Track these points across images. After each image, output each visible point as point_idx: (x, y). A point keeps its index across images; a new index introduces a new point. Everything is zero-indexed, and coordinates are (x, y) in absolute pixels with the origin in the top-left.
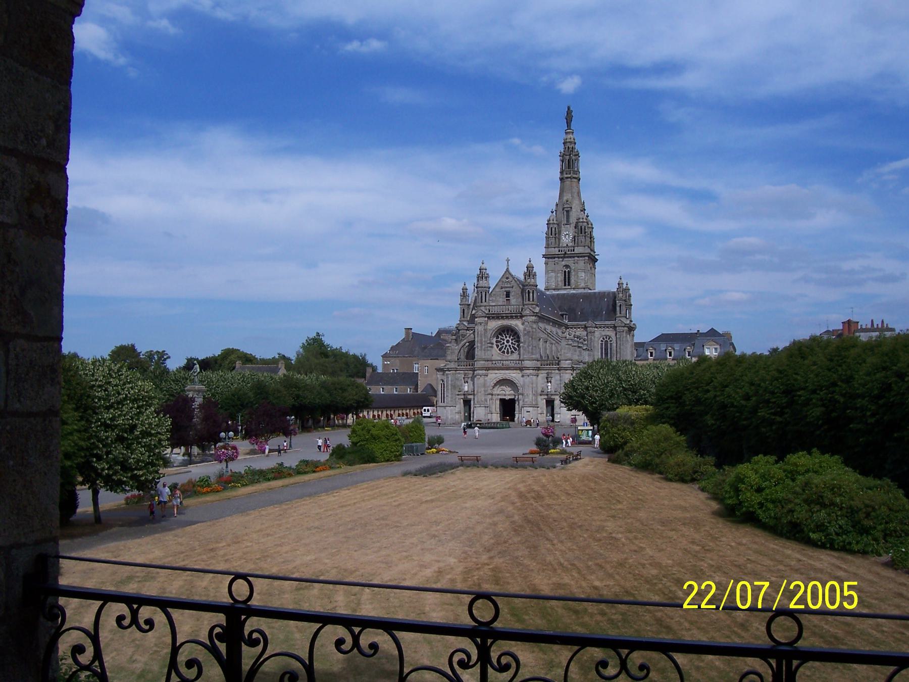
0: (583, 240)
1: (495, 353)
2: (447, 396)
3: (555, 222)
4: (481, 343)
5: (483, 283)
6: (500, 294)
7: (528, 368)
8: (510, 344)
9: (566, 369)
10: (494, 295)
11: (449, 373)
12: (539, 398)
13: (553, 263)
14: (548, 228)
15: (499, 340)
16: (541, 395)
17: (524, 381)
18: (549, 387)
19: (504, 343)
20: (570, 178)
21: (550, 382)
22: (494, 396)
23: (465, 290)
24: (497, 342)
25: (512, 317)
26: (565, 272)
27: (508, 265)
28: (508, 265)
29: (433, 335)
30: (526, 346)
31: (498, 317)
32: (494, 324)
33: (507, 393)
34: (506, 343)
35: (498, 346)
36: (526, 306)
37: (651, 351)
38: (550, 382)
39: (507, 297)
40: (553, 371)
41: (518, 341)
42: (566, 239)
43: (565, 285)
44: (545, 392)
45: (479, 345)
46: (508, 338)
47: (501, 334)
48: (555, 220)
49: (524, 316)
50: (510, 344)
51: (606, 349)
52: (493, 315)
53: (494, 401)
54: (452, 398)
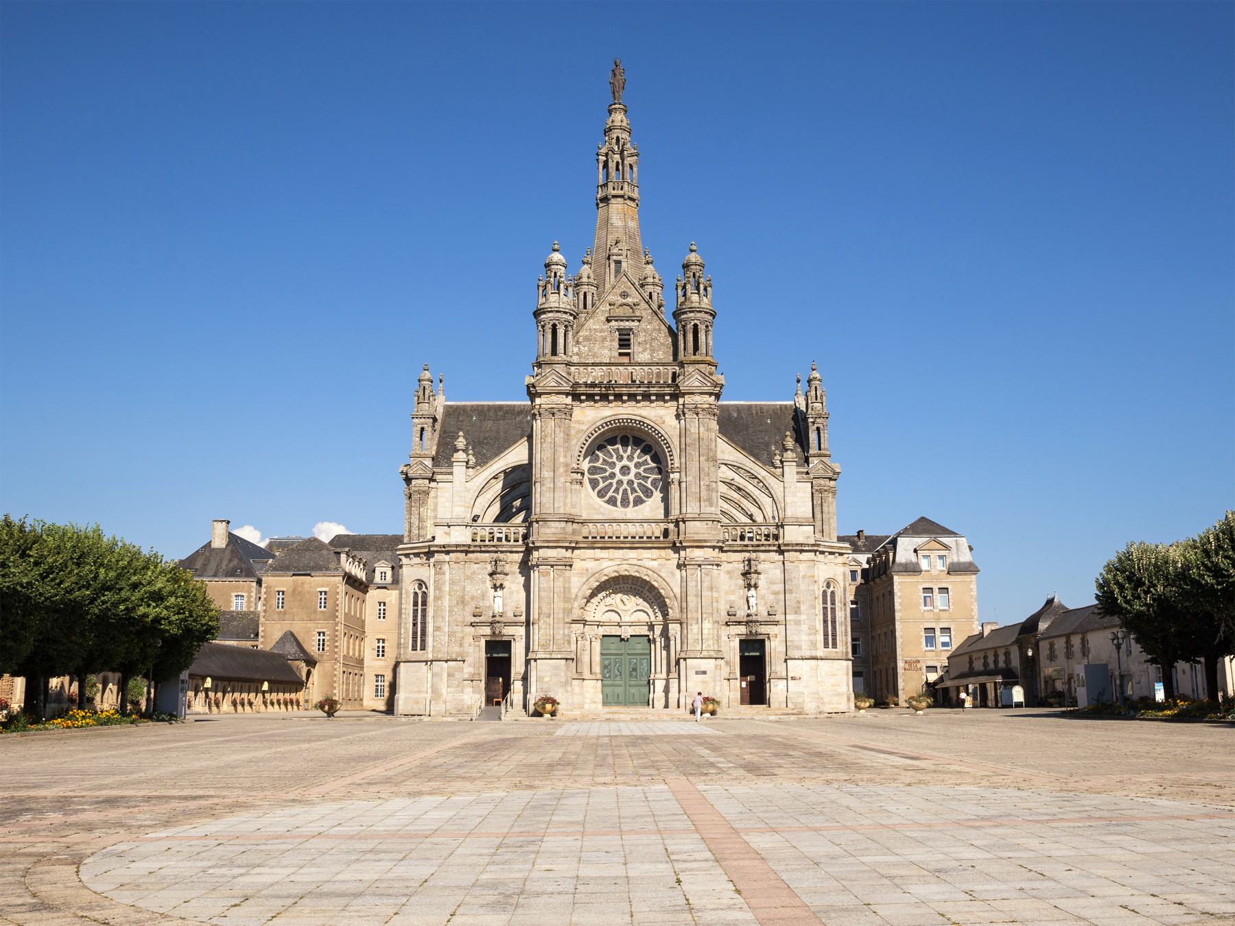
1: (588, 503)
2: (437, 629)
3: (591, 280)
6: (604, 339)
8: (631, 476)
9: (800, 548)
10: (587, 339)
11: (447, 558)
12: (725, 631)
16: (727, 624)
17: (684, 582)
18: (752, 601)
19: (613, 476)
20: (622, 197)
21: (756, 586)
24: (593, 470)
25: (646, 397)
31: (604, 393)
32: (591, 417)
33: (626, 618)
34: (619, 476)
35: (594, 484)
36: (690, 369)
39: (621, 346)
40: (762, 556)
44: (741, 614)
48: (592, 276)
49: (683, 395)
50: (631, 476)
52: (590, 391)
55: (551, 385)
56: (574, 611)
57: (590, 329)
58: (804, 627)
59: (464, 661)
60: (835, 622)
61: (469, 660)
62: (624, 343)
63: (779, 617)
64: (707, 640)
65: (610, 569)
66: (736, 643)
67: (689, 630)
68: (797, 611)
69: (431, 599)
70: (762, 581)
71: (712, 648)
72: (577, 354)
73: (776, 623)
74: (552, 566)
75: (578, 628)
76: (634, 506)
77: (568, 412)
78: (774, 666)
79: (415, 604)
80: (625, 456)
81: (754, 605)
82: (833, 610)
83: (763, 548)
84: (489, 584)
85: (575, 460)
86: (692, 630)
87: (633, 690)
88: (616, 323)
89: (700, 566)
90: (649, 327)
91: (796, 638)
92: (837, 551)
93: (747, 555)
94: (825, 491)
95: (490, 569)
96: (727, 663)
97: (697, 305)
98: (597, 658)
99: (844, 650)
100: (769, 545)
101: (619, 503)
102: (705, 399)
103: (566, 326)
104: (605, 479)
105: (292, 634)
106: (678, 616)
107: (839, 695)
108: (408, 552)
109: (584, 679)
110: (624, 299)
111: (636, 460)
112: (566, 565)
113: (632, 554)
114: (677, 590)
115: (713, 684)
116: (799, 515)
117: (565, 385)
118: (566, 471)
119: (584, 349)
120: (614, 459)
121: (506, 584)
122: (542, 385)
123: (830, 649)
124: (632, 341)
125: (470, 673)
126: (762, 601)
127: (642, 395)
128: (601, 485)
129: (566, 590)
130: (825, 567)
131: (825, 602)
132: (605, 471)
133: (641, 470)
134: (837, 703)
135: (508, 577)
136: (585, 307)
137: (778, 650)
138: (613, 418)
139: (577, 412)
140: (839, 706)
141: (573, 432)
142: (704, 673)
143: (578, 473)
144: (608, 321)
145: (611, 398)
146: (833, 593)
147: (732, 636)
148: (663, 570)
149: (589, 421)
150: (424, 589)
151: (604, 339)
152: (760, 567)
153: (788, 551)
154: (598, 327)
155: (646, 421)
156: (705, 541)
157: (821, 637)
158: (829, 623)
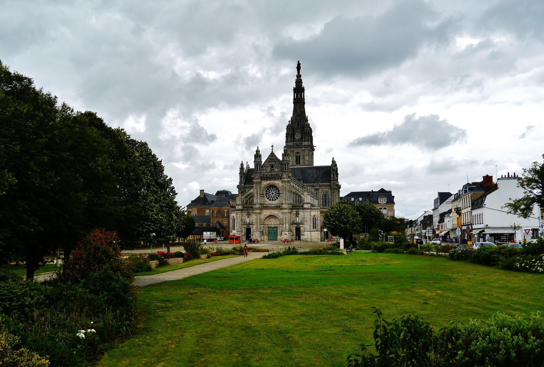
2: (237, 226)
4: (257, 194)
5: (258, 160)
6: (268, 166)
7: (285, 209)
8: (274, 195)
9: (307, 209)
10: (265, 166)
14: (287, 131)
18: (298, 220)
19: (270, 195)
20: (300, 102)
21: (298, 217)
23: (242, 165)
24: (266, 194)
25: (275, 179)
27: (272, 149)
28: (272, 149)
29: (214, 194)
32: (265, 183)
34: (271, 195)
35: (267, 196)
40: (300, 211)
41: (279, 193)
42: (298, 136)
43: (297, 164)
44: (295, 222)
45: (256, 195)
46: (273, 192)
47: (268, 189)
50: (274, 195)
51: (326, 199)
54: (239, 227)
58: (308, 225)
61: (243, 232)
62: (272, 166)
63: (303, 223)
66: (295, 228)
68: (307, 222)
69: (235, 220)
70: (300, 216)
73: (303, 224)
75: (263, 226)
77: (260, 183)
78: (302, 233)
82: (315, 221)
84: (246, 217)
87: (274, 237)
96: (293, 232)
98: (267, 231)
104: (269, 195)
105: (218, 222)
113: (273, 211)
114: (282, 218)
128: (268, 197)
129: (260, 218)
131: (313, 219)
139: (262, 182)
144: (269, 162)
146: (315, 218)
151: (268, 166)
152: (300, 213)
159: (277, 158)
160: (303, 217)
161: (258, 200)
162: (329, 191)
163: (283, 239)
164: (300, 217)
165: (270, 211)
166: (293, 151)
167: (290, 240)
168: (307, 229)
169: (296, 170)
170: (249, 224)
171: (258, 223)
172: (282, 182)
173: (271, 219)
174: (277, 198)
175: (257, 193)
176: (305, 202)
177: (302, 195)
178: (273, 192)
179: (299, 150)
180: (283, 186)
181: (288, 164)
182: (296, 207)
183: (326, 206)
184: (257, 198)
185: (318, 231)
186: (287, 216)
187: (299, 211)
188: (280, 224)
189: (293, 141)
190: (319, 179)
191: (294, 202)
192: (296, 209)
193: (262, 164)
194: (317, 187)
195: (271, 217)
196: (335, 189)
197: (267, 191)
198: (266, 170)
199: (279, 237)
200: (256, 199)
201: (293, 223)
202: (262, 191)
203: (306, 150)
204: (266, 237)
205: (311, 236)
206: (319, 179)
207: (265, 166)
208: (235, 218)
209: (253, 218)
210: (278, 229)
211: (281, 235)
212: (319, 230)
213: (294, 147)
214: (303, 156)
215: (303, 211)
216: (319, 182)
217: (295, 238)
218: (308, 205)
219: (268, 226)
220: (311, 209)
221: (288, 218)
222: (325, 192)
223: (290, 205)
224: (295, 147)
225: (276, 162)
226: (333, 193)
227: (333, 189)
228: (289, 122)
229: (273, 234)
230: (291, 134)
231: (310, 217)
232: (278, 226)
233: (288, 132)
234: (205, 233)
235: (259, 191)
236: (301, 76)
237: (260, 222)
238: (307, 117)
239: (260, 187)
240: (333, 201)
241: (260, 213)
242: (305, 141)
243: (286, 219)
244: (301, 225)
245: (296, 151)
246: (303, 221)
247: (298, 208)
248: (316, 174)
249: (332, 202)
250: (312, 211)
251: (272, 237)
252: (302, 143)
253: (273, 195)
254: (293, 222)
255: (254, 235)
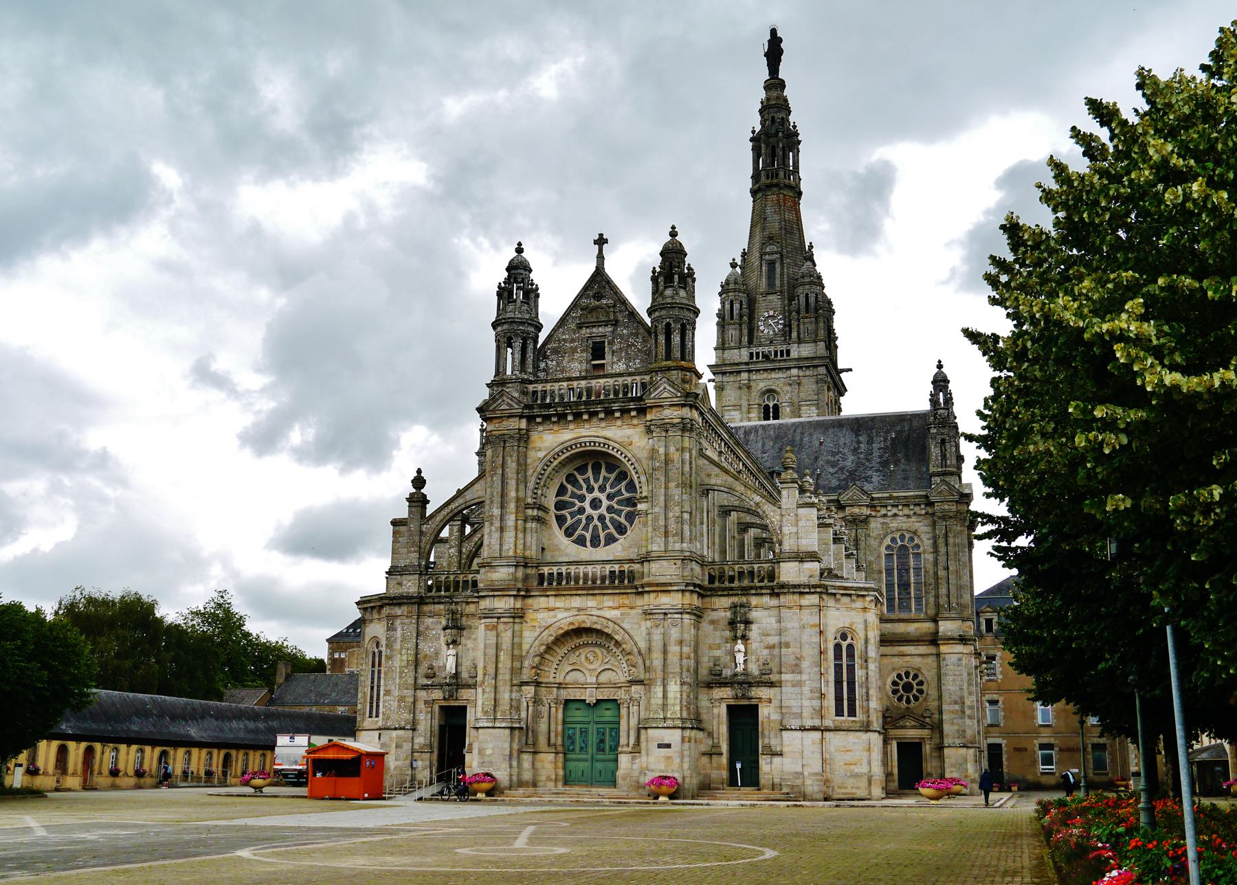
0: (811, 327)
4: (502, 507)
7: (663, 588)
8: (603, 510)
9: (798, 589)
13: (737, 385)
14: (723, 303)
15: (566, 498)
18: (740, 658)
19: (582, 510)
20: (777, 185)
21: (744, 638)
22: (543, 691)
24: (560, 506)
25: (609, 413)
26: (767, 407)
27: (600, 257)
28: (600, 257)
30: (656, 509)
34: (589, 511)
35: (561, 520)
37: (988, 616)
38: (744, 638)
40: (754, 601)
42: (769, 326)
44: (727, 673)
45: (496, 511)
46: (596, 494)
47: (571, 479)
50: (603, 510)
53: (544, 710)
54: (402, 699)
55: (502, 408)
56: (525, 671)
57: (559, 340)
58: (806, 690)
59: (414, 730)
60: (854, 683)
62: (598, 351)
63: (774, 677)
64: (674, 705)
65: (564, 621)
66: (723, 710)
67: (652, 694)
68: (796, 668)
70: (754, 632)
71: (679, 716)
72: (544, 370)
73: (771, 684)
74: (499, 618)
75: (529, 691)
76: (605, 546)
77: (523, 438)
78: (768, 738)
79: (373, 666)
80: (596, 486)
81: (742, 662)
82: (851, 669)
83: (753, 592)
84: (443, 640)
85: (530, 493)
86: (655, 693)
87: (599, 766)
88: (588, 331)
89: (665, 614)
90: (625, 332)
91: (793, 703)
92: (853, 592)
93: (735, 599)
94: (950, 518)
95: (444, 623)
97: (669, 300)
99: (865, 719)
100: (761, 588)
101: (588, 543)
102: (675, 413)
103: (525, 340)
104: (572, 515)
106: (642, 677)
107: (856, 776)
108: (365, 606)
109: (535, 753)
110: (598, 301)
111: (608, 490)
112: (514, 617)
113: (591, 602)
114: (642, 645)
115: (678, 760)
116: (803, 549)
117: (516, 406)
118: (517, 507)
119: (551, 364)
120: (584, 491)
121: (463, 640)
122: (491, 408)
123: (845, 718)
124: (606, 349)
125: (420, 744)
126: (753, 657)
127: (557, 415)
128: (569, 521)
129: (516, 645)
130: (837, 613)
131: (838, 656)
132: (573, 505)
133: (613, 503)
134: (852, 788)
135: (465, 633)
136: (732, 318)
137: (772, 718)
138: (573, 442)
139: (534, 436)
140: (854, 791)
141: (529, 461)
142: (668, 746)
143: (533, 508)
145: (570, 418)
146: (850, 647)
147: (716, 700)
148: (626, 620)
149: (546, 448)
150: (380, 648)
151: (574, 350)
152: (754, 615)
153: (785, 593)
154: (567, 336)
155: (611, 443)
156: (670, 584)
157: (830, 701)
158: (845, 684)
159: (623, 302)
160: (773, 640)
161: (510, 536)
162: (922, 527)
163: (647, 780)
164: (754, 645)
165: (577, 602)
166: (749, 387)
167: (691, 782)
168: (800, 716)
169: (752, 436)
170: (456, 683)
171: (505, 675)
172: (649, 431)
173: (584, 652)
174: (621, 530)
175: (503, 495)
176: (787, 547)
177: (768, 508)
178: (596, 494)
179: (776, 380)
180: (653, 451)
181: (683, 326)
182: (732, 579)
183: (905, 607)
184: (502, 529)
185: (866, 728)
186: (675, 633)
187: (747, 606)
188: (633, 682)
189: (750, 342)
190: (870, 473)
191: (723, 552)
192: (728, 592)
193: (541, 341)
194: (856, 510)
195: (585, 639)
196: (955, 517)
197: (562, 491)
198: (562, 371)
199: (624, 760)
200: (496, 535)
201: (716, 680)
202: (531, 485)
203: (804, 381)
204: (548, 763)
205: (823, 761)
206: (870, 473)
207: (556, 351)
208: (383, 649)
209: (479, 639)
210: (624, 711)
211: (636, 750)
212: (876, 724)
213: (752, 367)
214: (792, 404)
215: (774, 602)
216: (867, 487)
217: (725, 774)
218: (808, 565)
219: (565, 694)
220: (821, 590)
221: (681, 643)
222: (902, 537)
223: (697, 568)
224: (760, 366)
225: (616, 323)
226: (941, 541)
227: (944, 518)
228: (734, 265)
229: (592, 749)
230: (741, 316)
231: (816, 639)
232: (621, 695)
233: (727, 306)
234: (282, 740)
235: (512, 484)
236: (782, 85)
237: (514, 671)
238: (811, 247)
239: (522, 466)
240: (943, 583)
241: (518, 616)
242: (800, 341)
243: (665, 652)
244: (763, 692)
245: (762, 385)
246: (774, 665)
247: (746, 583)
248: (855, 451)
249: (937, 587)
250: (830, 602)
251: (582, 765)
252: (788, 352)
253: (595, 514)
254: (711, 672)
255: (475, 751)
